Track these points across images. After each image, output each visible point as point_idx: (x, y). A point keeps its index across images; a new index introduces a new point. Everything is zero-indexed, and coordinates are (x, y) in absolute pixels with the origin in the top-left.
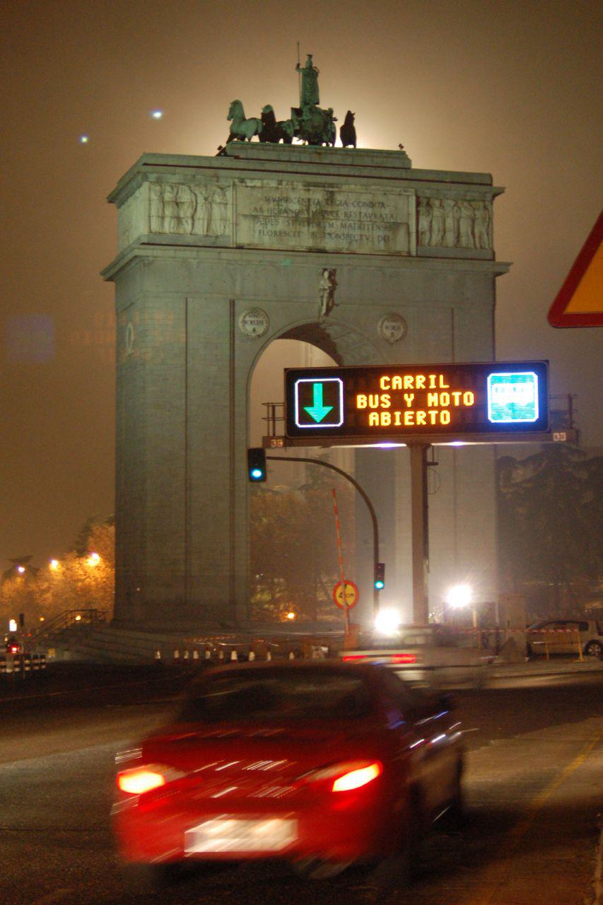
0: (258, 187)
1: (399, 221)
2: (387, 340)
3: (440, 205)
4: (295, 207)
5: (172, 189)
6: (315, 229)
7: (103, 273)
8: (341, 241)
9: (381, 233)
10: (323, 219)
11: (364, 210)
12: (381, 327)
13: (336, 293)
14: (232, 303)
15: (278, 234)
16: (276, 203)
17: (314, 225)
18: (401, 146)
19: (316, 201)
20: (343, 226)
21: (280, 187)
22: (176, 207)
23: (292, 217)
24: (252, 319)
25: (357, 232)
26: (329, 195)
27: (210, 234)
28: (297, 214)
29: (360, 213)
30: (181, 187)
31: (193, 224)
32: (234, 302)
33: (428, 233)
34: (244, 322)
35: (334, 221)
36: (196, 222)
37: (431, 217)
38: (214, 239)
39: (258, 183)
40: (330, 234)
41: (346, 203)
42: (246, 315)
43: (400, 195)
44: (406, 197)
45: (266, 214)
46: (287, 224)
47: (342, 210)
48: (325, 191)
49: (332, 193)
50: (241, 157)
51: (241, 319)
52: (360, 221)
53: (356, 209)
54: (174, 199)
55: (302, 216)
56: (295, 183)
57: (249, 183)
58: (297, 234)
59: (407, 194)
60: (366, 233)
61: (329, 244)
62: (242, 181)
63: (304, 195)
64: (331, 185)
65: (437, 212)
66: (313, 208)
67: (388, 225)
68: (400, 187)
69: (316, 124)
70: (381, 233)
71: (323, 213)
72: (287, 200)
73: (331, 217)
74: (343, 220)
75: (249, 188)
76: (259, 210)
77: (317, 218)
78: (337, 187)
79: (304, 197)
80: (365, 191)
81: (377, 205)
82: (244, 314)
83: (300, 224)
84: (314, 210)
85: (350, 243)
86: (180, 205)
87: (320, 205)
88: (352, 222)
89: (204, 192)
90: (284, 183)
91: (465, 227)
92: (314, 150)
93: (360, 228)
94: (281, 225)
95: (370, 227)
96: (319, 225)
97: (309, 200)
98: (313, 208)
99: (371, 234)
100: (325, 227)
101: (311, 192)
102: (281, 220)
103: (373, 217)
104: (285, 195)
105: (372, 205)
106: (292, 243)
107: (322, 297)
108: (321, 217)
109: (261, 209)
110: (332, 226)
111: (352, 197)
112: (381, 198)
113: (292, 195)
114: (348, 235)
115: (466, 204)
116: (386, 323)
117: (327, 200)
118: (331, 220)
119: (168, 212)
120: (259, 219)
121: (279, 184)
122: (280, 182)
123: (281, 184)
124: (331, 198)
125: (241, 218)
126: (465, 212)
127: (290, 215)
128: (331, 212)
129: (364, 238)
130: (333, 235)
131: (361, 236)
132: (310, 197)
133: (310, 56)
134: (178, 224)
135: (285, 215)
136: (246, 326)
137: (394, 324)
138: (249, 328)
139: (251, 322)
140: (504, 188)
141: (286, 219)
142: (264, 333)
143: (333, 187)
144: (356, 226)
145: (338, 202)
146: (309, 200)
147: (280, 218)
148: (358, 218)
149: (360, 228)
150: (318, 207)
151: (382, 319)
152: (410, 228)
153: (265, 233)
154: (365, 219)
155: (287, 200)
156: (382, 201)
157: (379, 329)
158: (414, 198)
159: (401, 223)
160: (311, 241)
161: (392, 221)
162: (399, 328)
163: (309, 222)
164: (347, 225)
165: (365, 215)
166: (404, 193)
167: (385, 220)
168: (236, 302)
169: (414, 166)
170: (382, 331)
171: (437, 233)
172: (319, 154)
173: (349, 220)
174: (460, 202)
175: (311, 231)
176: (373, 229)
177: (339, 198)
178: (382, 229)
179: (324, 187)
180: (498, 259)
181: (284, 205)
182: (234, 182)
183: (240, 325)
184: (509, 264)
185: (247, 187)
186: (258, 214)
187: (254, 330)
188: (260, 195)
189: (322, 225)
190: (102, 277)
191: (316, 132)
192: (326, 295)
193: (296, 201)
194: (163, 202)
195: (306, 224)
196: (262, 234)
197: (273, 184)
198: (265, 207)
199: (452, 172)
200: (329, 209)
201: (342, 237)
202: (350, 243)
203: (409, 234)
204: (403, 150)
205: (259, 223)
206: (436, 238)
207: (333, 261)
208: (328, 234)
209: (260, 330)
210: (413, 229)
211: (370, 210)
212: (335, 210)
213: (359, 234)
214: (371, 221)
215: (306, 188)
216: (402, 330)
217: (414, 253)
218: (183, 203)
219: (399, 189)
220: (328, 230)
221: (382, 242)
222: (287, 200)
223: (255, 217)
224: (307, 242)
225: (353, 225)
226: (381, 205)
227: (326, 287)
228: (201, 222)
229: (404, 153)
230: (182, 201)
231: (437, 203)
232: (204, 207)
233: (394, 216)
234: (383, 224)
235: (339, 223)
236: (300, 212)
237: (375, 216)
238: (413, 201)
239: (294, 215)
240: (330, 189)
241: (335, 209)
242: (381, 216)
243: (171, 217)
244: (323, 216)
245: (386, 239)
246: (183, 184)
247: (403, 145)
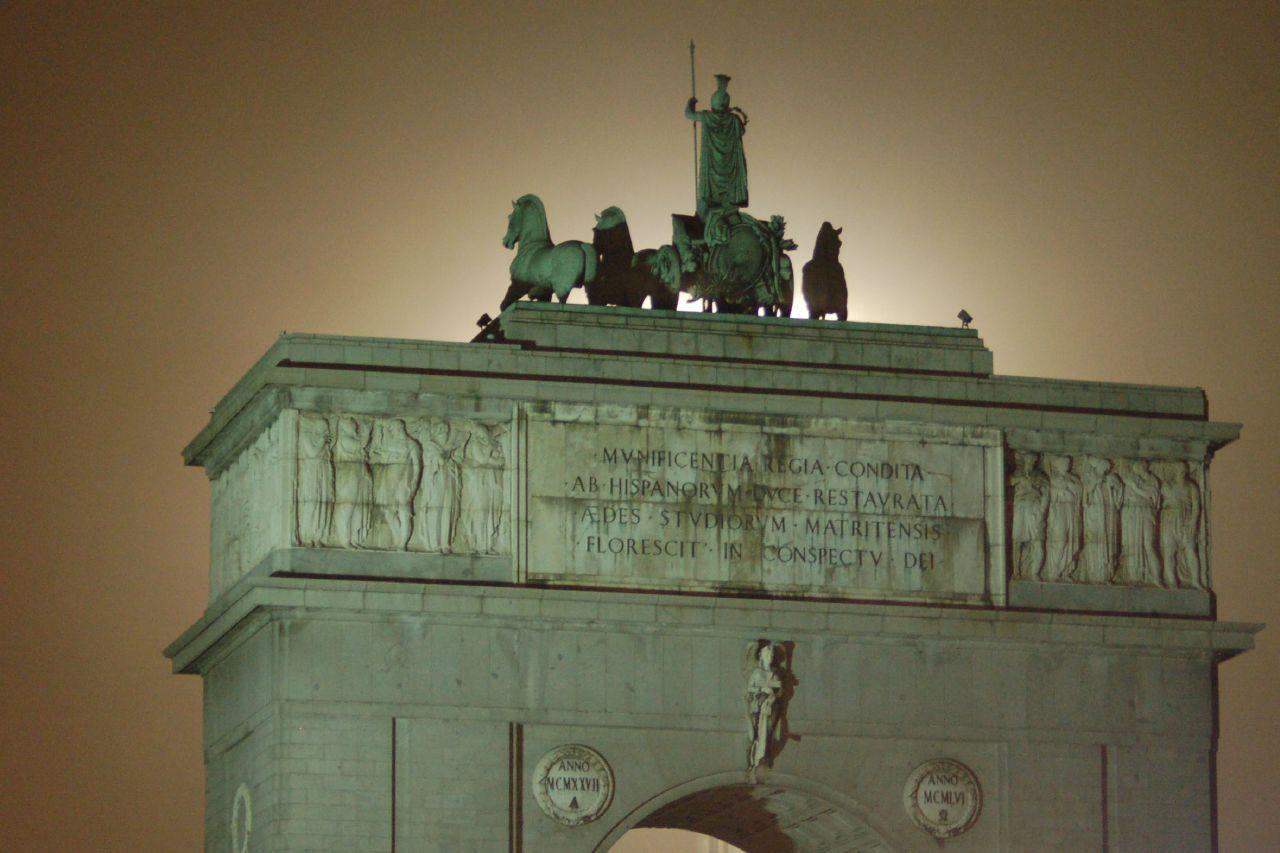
0: (588, 424)
1: (960, 514)
2: (931, 831)
3: (1070, 471)
4: (683, 476)
5: (357, 429)
7: (172, 652)
8: (806, 565)
9: (913, 546)
10: (758, 508)
11: (867, 484)
13: (793, 705)
14: (517, 733)
15: (638, 547)
16: (632, 465)
17: (735, 524)
18: (965, 317)
19: (739, 464)
21: (643, 423)
22: (367, 477)
23: (677, 504)
24: (569, 774)
25: (849, 542)
26: (773, 444)
27: (456, 549)
28: (689, 497)
29: (857, 494)
30: (378, 422)
31: (412, 523)
32: (520, 728)
33: (1037, 545)
34: (548, 783)
35: (786, 514)
36: (421, 515)
37: (1044, 503)
38: (468, 561)
39: (586, 414)
40: (776, 550)
41: (818, 466)
42: (553, 764)
43: (963, 444)
44: (978, 452)
45: (605, 494)
46: (662, 520)
47: (809, 483)
48: (763, 433)
49: (782, 439)
50: (540, 343)
51: (538, 774)
52: (856, 513)
53: (846, 483)
54: (361, 456)
55: (704, 500)
56: (683, 413)
57: (561, 413)
58: (688, 548)
59: (982, 442)
60: (871, 544)
61: (776, 575)
62: (543, 407)
63: (710, 446)
64: (780, 419)
65: (1060, 490)
66: (732, 480)
67: (930, 524)
68: (963, 425)
69: (739, 258)
70: (913, 546)
71: (758, 493)
72: (661, 457)
73: (777, 503)
74: (811, 512)
75: (562, 426)
76: (586, 482)
78: (795, 424)
80: (868, 435)
81: (902, 472)
82: (545, 762)
83: (696, 524)
84: (735, 486)
85: (830, 573)
86: (377, 471)
87: (750, 470)
88: (835, 517)
89: (441, 438)
90: (654, 412)
92: (733, 326)
93: (855, 531)
94: (647, 523)
95: (884, 529)
96: (747, 524)
97: (720, 457)
98: (732, 480)
99: (885, 548)
100: (762, 530)
101: (726, 437)
102: (645, 511)
103: (891, 500)
104: (656, 445)
105: (888, 470)
106: (674, 571)
107: (757, 715)
108: (754, 504)
109: (594, 485)
110: (781, 526)
111: (836, 452)
112: (913, 455)
113: (677, 445)
114: (824, 553)
115: (1137, 468)
116: (926, 787)
117: (768, 458)
118: (780, 510)
119: (347, 488)
120: (588, 508)
121: (639, 417)
122: (644, 411)
123: (647, 416)
124: (778, 453)
125: (541, 506)
126: (1136, 491)
127: (671, 498)
128: (779, 491)
129: (867, 558)
130: (784, 552)
131: (860, 553)
132: (724, 449)
133: (724, 80)
134: (373, 520)
135: (657, 497)
136: (554, 794)
137: (946, 788)
139: (567, 785)
140: (1240, 426)
141: (660, 510)
142: (601, 813)
143: (783, 424)
144: (847, 527)
145: (797, 464)
146: (720, 457)
147: (643, 505)
148: (851, 506)
149: (856, 531)
150: (746, 476)
151: (915, 776)
152: (991, 532)
153: (604, 546)
154: (870, 508)
155: (661, 457)
156: (917, 462)
157: (908, 803)
158: (999, 452)
159: (966, 520)
160: (725, 565)
161: (941, 513)
162: (961, 797)
164: (822, 524)
166: (975, 441)
167: (923, 512)
168: (526, 730)
169: (999, 369)
170: (915, 805)
171: (1060, 545)
172: (749, 336)
173: (826, 511)
174: (1120, 463)
175: (725, 538)
176: (889, 536)
177: (801, 452)
178: (915, 533)
179: (760, 422)
180: (1223, 615)
181: (653, 471)
182: (521, 411)
183: (537, 789)
184: (1252, 629)
185: (554, 422)
186: (586, 494)
187: (574, 804)
188: (589, 445)
189: (755, 524)
190: (169, 662)
191: (739, 278)
192: (766, 710)
193: (686, 460)
194: (332, 462)
195: (712, 521)
196: (594, 548)
197: (627, 415)
198: (604, 475)
199: (1100, 385)
200: (774, 483)
201: (809, 557)
202: (830, 573)
203: (987, 548)
204: (971, 326)
205: (588, 518)
207: (785, 622)
208: (773, 548)
209: (591, 803)
210: (997, 534)
211: (882, 486)
212: (789, 485)
213: (854, 548)
214: (883, 514)
215: (714, 427)
216: (970, 803)
217: (1000, 601)
218: (385, 466)
219: (959, 430)
220: (771, 538)
221: (916, 570)
222: (660, 460)
223: (576, 504)
224: (716, 569)
225: (837, 525)
226: (911, 473)
227: (767, 690)
228: (433, 515)
229: (973, 334)
230: (384, 460)
231: (1061, 466)
232: (441, 477)
233: (948, 506)
234: (919, 520)
235: (801, 519)
236: (698, 489)
238: (997, 458)
239: (681, 496)
240: (778, 430)
241: (790, 481)
242: (913, 499)
243: (355, 504)
244: (759, 501)
245: (924, 562)
246: (385, 416)
247: (971, 313)
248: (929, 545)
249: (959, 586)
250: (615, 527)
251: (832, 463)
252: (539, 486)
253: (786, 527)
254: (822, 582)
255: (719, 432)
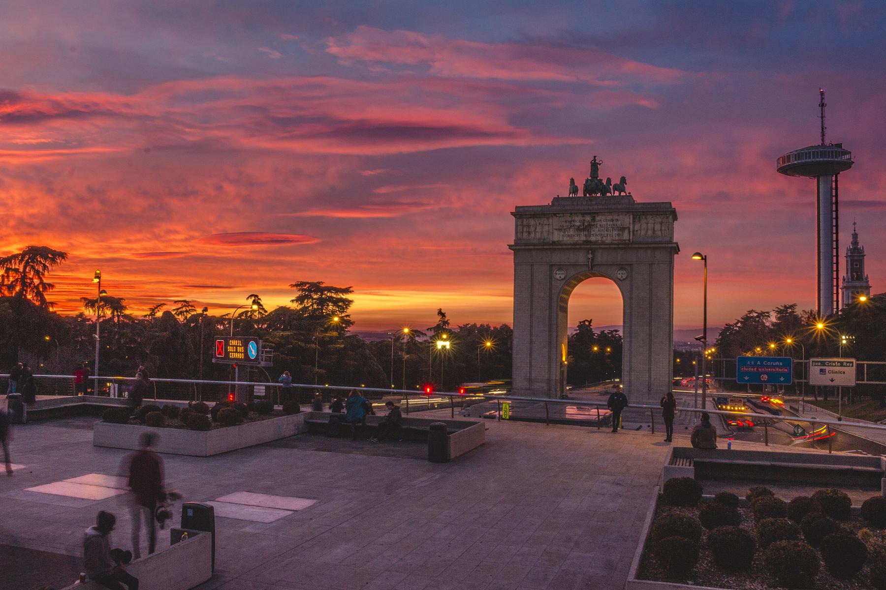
2: (619, 279)
4: (578, 224)
6: (586, 233)
9: (616, 232)
11: (609, 223)
12: (617, 273)
20: (599, 230)
25: (606, 233)
28: (579, 227)
40: (593, 235)
47: (599, 224)
57: (558, 215)
60: (608, 233)
61: (593, 239)
64: (594, 213)
66: (586, 224)
70: (616, 232)
71: (590, 226)
72: (574, 221)
75: (558, 218)
77: (586, 228)
79: (581, 219)
91: (657, 227)
94: (572, 232)
98: (586, 224)
102: (571, 230)
104: (573, 219)
105: (612, 220)
109: (563, 226)
110: (594, 231)
111: (603, 217)
112: (617, 217)
116: (619, 272)
119: (525, 229)
124: (594, 219)
125: (555, 231)
128: (594, 225)
129: (608, 235)
131: (607, 234)
138: (558, 276)
142: (564, 278)
144: (605, 230)
146: (584, 220)
155: (574, 221)
163: (584, 230)
165: (609, 225)
177: (598, 218)
187: (560, 277)
198: (565, 224)
200: (593, 224)
203: (629, 232)
206: (643, 233)
209: (563, 276)
211: (611, 223)
218: (530, 226)
223: (560, 230)
229: (631, 196)
235: (597, 229)
236: (580, 226)
237: (614, 225)
241: (596, 223)
244: (590, 227)
245: (618, 235)
248: (619, 232)
249: (624, 239)
250: (566, 233)
251: (602, 220)
252: (555, 228)
253: (595, 231)
254: (600, 239)
255: (584, 216)
